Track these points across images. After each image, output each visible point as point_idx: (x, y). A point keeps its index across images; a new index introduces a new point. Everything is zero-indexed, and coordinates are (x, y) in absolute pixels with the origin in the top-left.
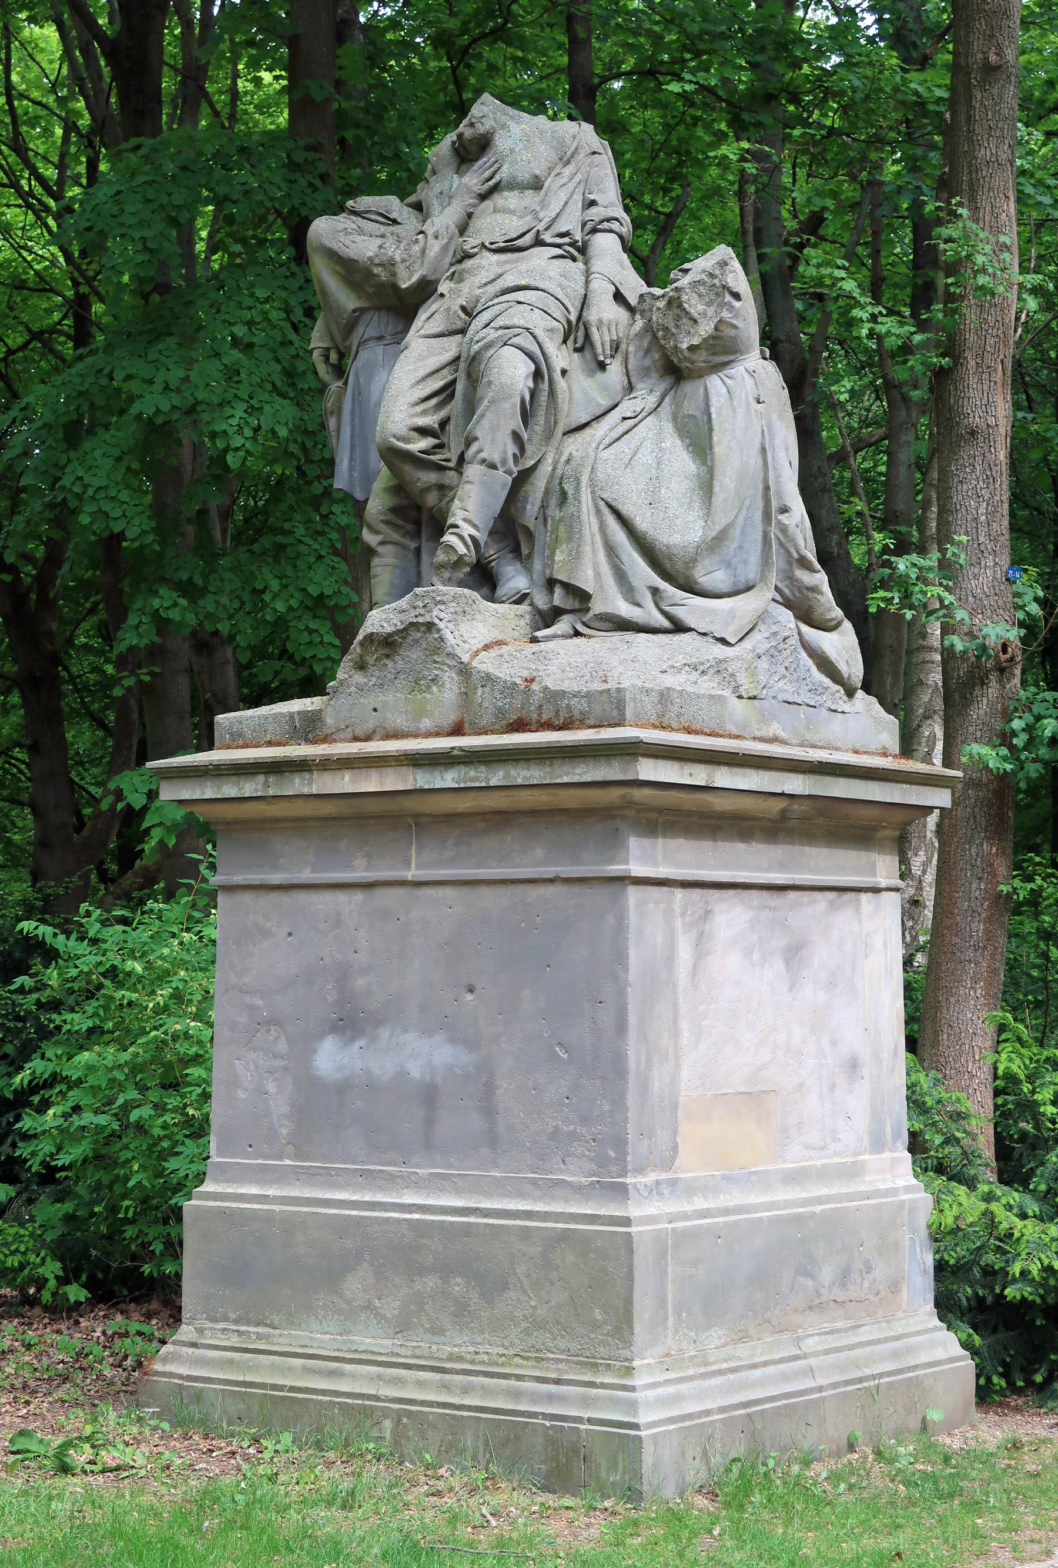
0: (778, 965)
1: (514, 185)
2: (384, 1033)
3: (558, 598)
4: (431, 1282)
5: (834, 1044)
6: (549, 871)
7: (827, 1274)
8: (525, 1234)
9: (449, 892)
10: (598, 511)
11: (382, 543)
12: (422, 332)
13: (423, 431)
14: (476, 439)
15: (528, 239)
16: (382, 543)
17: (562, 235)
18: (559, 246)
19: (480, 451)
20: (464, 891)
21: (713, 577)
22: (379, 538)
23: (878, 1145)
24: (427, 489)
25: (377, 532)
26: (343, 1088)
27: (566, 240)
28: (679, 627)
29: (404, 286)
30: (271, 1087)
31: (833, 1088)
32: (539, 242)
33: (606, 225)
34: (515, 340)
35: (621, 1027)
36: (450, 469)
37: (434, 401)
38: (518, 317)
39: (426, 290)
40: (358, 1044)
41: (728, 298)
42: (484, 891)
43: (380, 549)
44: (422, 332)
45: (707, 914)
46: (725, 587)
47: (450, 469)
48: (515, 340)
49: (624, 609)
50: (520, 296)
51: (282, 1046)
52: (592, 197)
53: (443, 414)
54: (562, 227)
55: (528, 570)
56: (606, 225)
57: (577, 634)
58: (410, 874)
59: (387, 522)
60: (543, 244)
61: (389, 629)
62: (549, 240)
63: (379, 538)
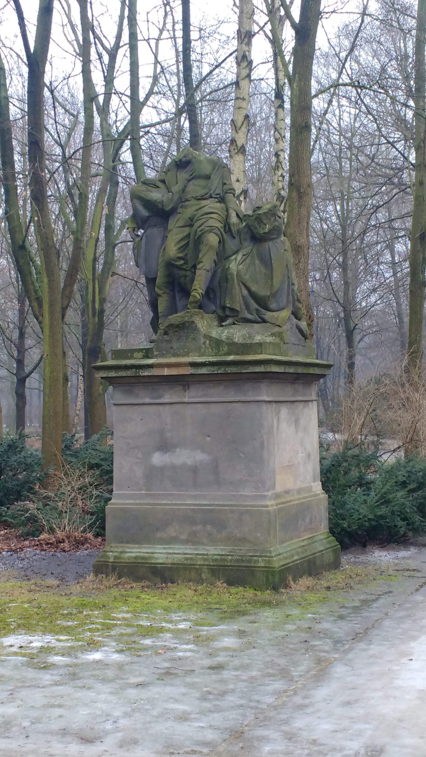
0: (293, 425)
1: (199, 177)
2: (178, 450)
3: (228, 313)
4: (200, 527)
5: (305, 449)
6: (237, 399)
7: (307, 520)
8: (232, 512)
9: (199, 405)
10: (239, 285)
11: (163, 293)
12: (176, 226)
13: (180, 258)
14: (202, 262)
15: (208, 196)
16: (163, 293)
17: (217, 194)
18: (216, 198)
19: (204, 266)
20: (206, 405)
21: (273, 306)
22: (162, 292)
23: (314, 481)
24: (181, 277)
25: (162, 290)
26: (162, 469)
27: (219, 196)
28: (264, 321)
29: (167, 209)
30: (136, 469)
31: (305, 463)
32: (211, 197)
33: (229, 191)
34: (214, 231)
35: (262, 447)
36: (188, 270)
37: (182, 249)
38: (212, 223)
39: (173, 211)
40: (168, 454)
41: (277, 218)
42: (212, 405)
43: (163, 295)
44: (176, 226)
45: (279, 411)
46: (276, 309)
47: (188, 270)
48: (214, 231)
49: (250, 317)
50: (212, 216)
51: (140, 455)
52: (225, 182)
53: (185, 253)
54: (217, 192)
55: (215, 304)
56: (229, 191)
57: (234, 324)
58: (186, 400)
59: (165, 287)
60: (212, 197)
61: (177, 323)
62: (214, 196)
63: (162, 292)
